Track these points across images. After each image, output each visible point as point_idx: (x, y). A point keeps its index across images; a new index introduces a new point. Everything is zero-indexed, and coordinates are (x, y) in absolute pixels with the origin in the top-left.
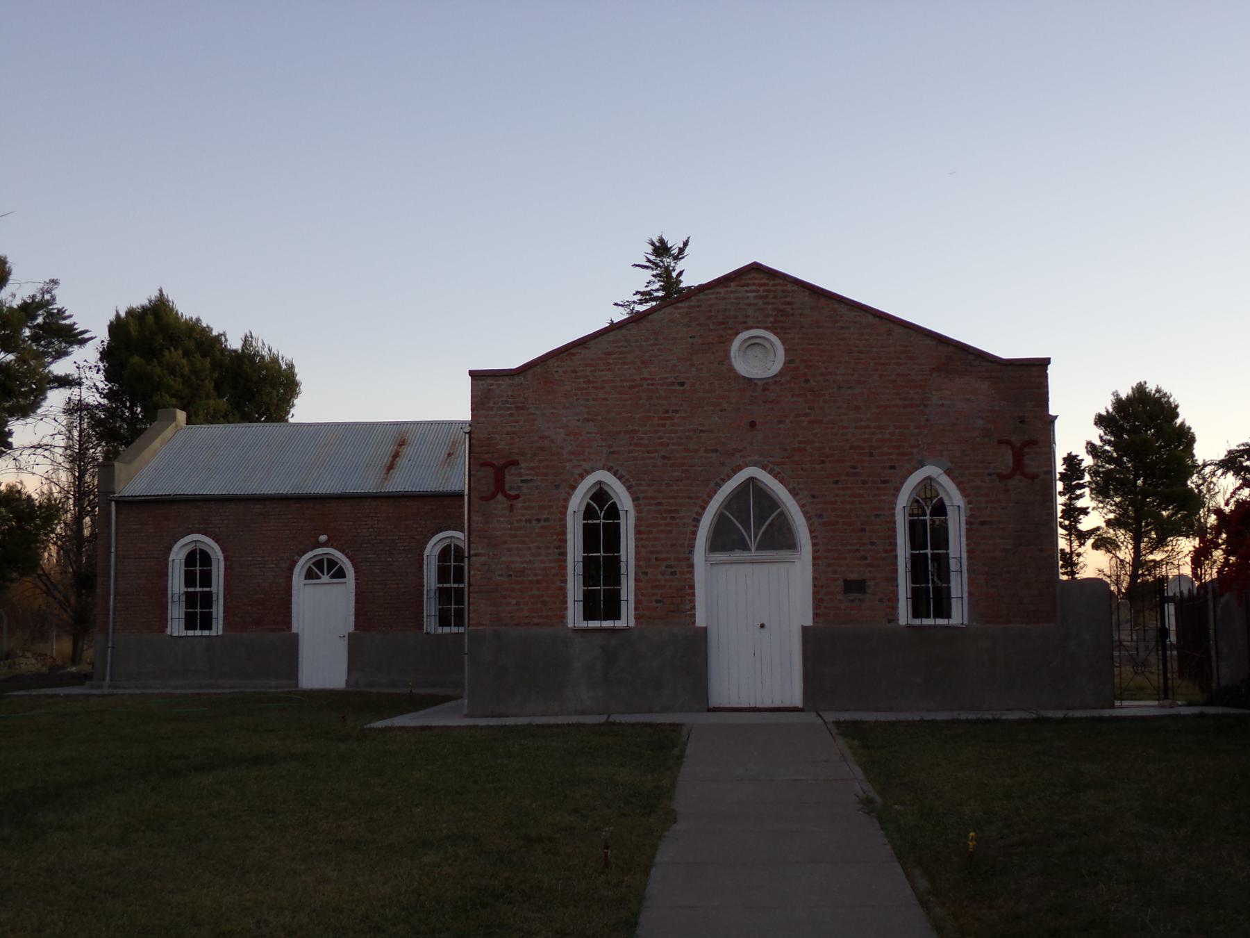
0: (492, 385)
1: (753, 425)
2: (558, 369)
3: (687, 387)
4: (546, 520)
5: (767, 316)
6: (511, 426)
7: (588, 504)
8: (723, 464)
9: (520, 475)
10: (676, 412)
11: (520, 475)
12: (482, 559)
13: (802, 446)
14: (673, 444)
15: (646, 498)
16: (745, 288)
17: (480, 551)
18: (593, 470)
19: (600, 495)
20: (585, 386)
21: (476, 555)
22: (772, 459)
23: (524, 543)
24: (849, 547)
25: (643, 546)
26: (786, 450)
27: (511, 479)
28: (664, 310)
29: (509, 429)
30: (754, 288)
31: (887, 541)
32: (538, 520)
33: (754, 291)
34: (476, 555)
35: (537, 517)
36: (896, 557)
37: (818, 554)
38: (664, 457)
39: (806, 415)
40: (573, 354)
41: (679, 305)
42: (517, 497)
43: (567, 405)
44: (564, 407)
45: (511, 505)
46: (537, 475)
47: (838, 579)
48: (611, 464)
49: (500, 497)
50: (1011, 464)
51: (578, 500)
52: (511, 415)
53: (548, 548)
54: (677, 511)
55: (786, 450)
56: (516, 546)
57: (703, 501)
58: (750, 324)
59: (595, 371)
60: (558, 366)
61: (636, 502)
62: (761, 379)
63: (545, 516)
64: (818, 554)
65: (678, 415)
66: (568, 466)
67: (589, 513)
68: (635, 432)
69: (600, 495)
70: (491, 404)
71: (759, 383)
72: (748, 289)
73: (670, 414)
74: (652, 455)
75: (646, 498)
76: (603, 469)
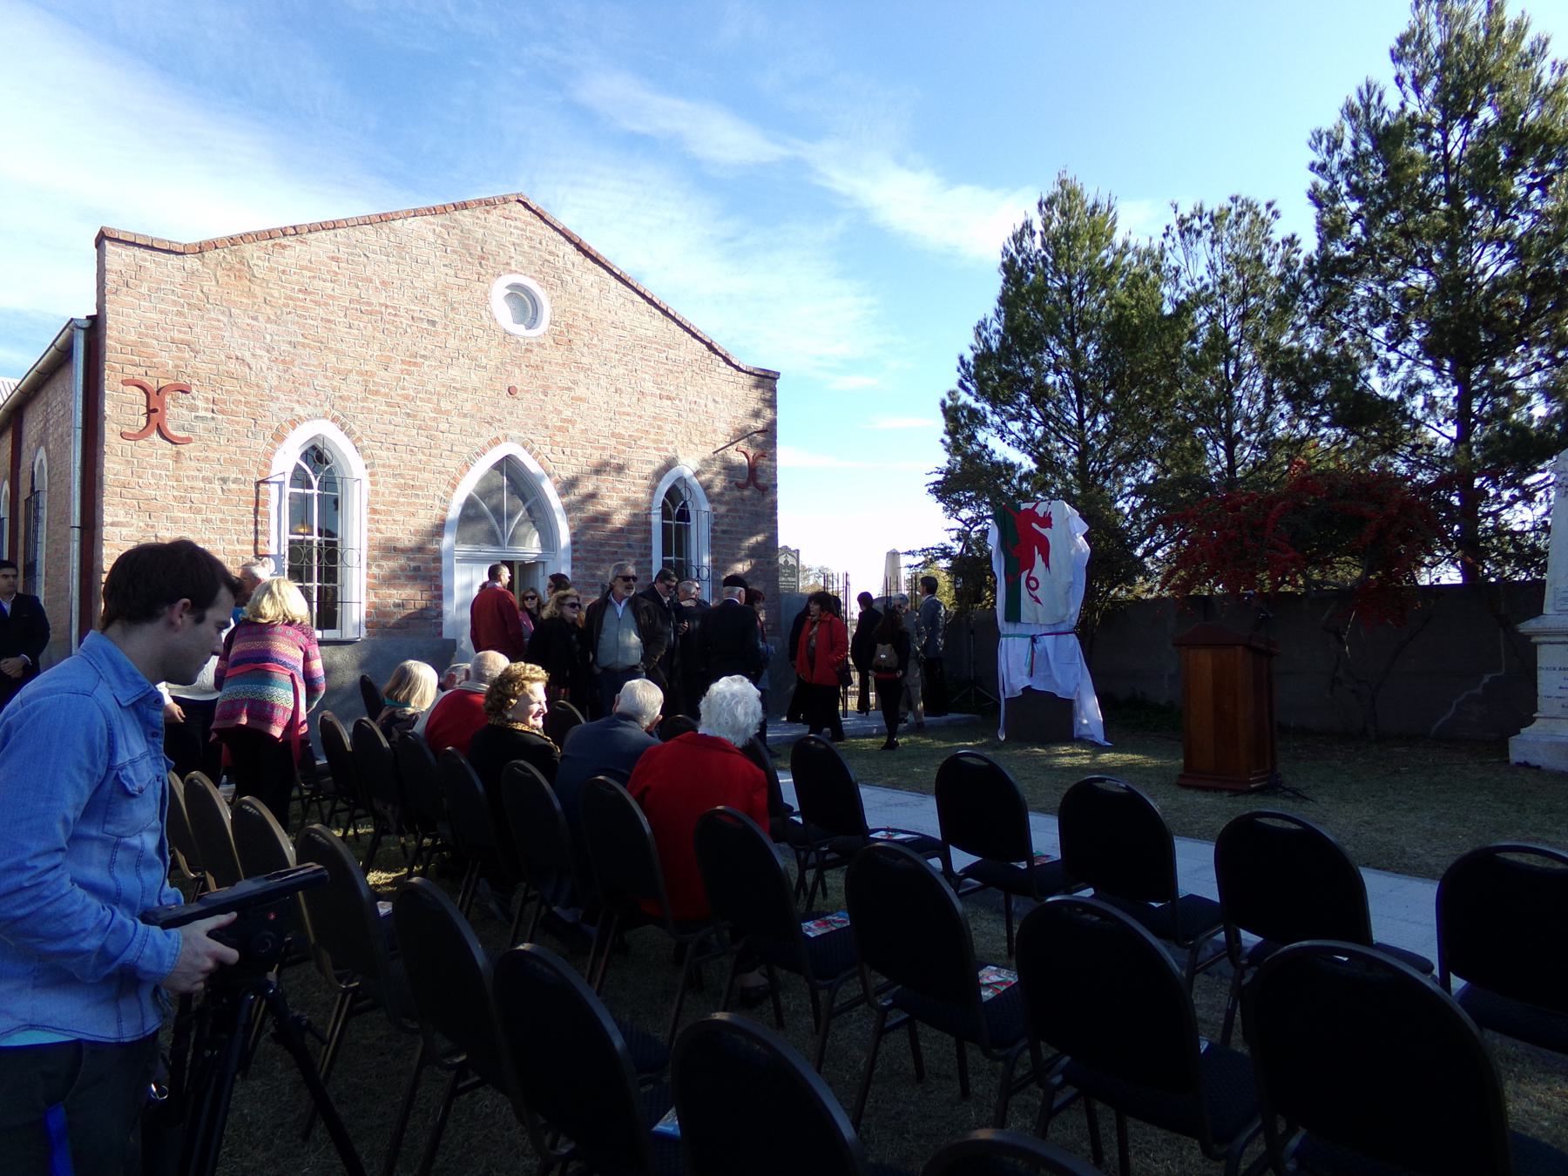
0: (145, 260)
1: (511, 391)
2: (261, 263)
3: (439, 328)
4: (236, 481)
5: (531, 263)
6: (180, 331)
7: (298, 468)
8: (478, 435)
9: (193, 408)
10: (423, 357)
11: (193, 408)
12: (125, 531)
13: (565, 425)
14: (421, 400)
15: (384, 466)
16: (509, 222)
17: (122, 519)
18: (309, 418)
19: (316, 455)
20: (301, 296)
21: (113, 524)
22: (532, 437)
23: (199, 511)
24: (607, 549)
25: (378, 530)
26: (547, 427)
27: (176, 414)
28: (410, 220)
29: (177, 336)
30: (519, 224)
31: (643, 544)
32: (224, 480)
33: (516, 227)
34: (113, 524)
35: (220, 475)
36: (651, 562)
37: (578, 554)
38: (408, 415)
39: (569, 389)
40: (284, 247)
41: (430, 218)
42: (188, 440)
43: (272, 317)
44: (269, 320)
45: (178, 453)
46: (222, 412)
47: (596, 585)
48: (336, 414)
49: (155, 437)
50: (747, 475)
51: (287, 458)
52: (179, 314)
53: (238, 522)
54: (421, 488)
55: (547, 427)
56: (186, 515)
57: (454, 478)
58: (513, 267)
59: (314, 277)
60: (259, 258)
61: (369, 470)
62: (524, 338)
63: (234, 476)
64: (578, 554)
65: (427, 363)
66: (274, 406)
67: (300, 479)
68: (373, 375)
69: (316, 455)
70: (144, 290)
71: (521, 340)
72: (513, 223)
73: (419, 360)
74: (392, 410)
75: (384, 466)
76: (325, 417)
